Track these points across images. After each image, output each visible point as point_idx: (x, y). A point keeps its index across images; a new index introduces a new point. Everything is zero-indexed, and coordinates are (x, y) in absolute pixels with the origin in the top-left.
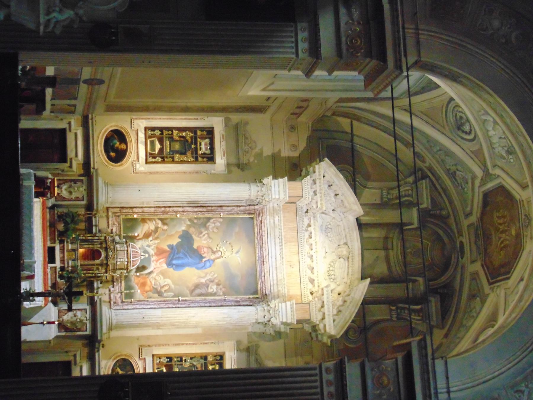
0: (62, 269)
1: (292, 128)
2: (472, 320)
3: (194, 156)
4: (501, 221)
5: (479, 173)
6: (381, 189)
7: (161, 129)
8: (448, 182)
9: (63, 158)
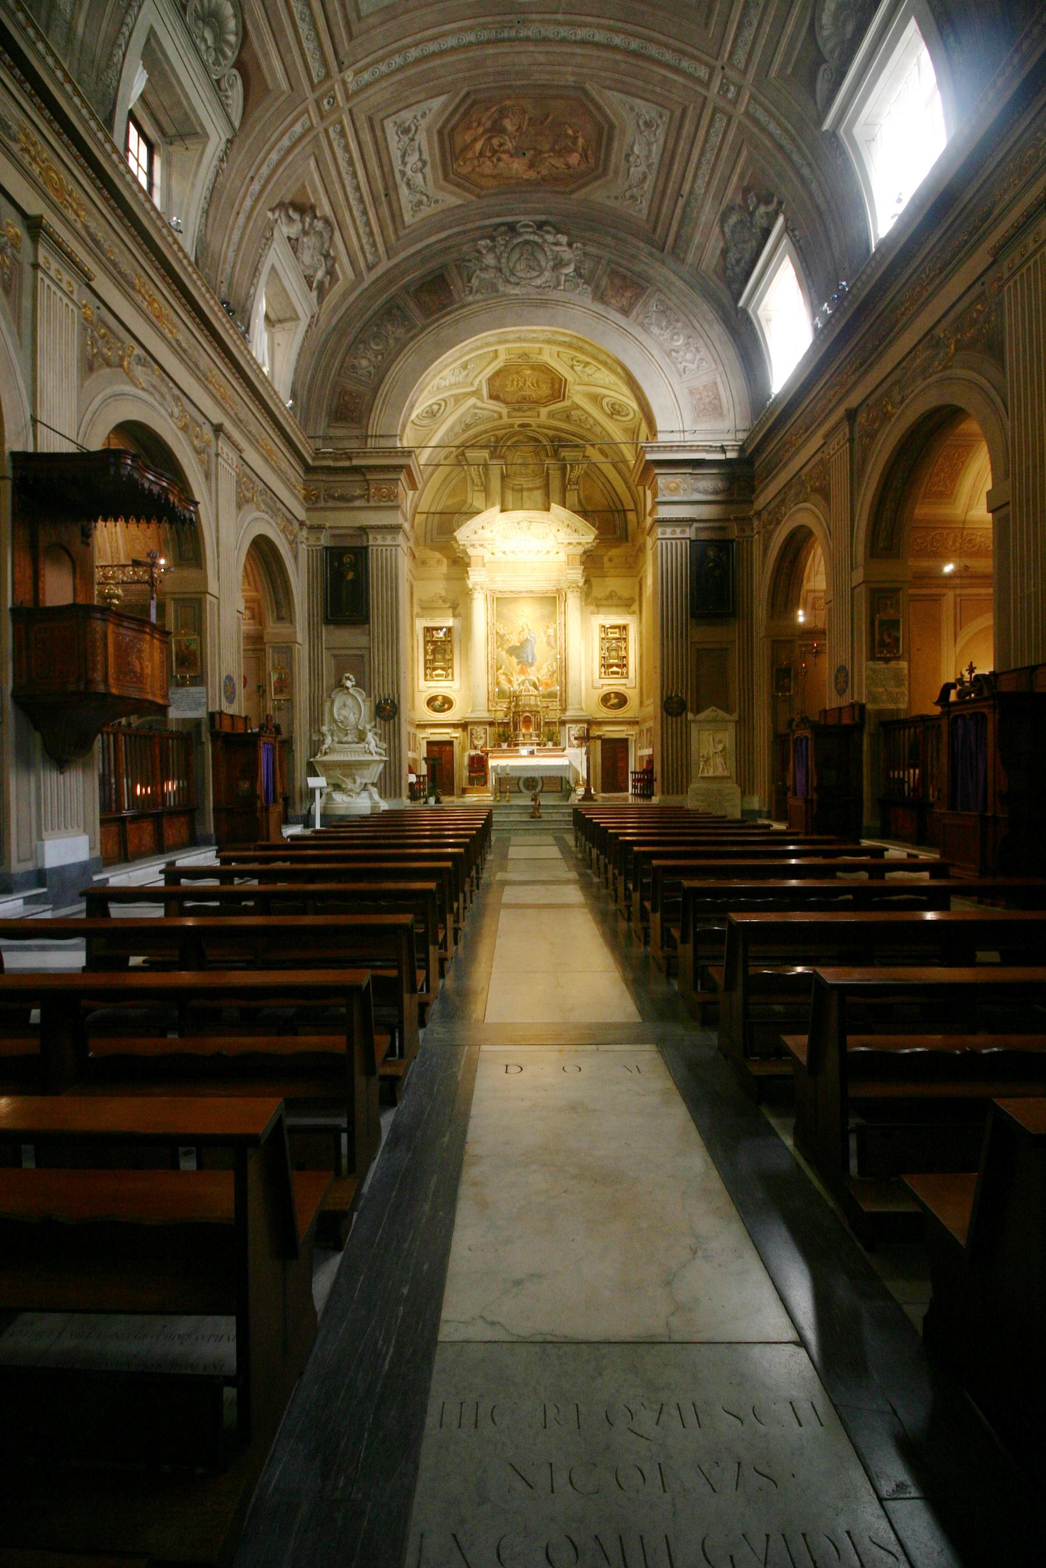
0: (538, 744)
1: (424, 563)
2: (590, 419)
4: (515, 383)
5: (473, 401)
6: (473, 491)
7: (426, 668)
8: (471, 432)
9: (450, 743)
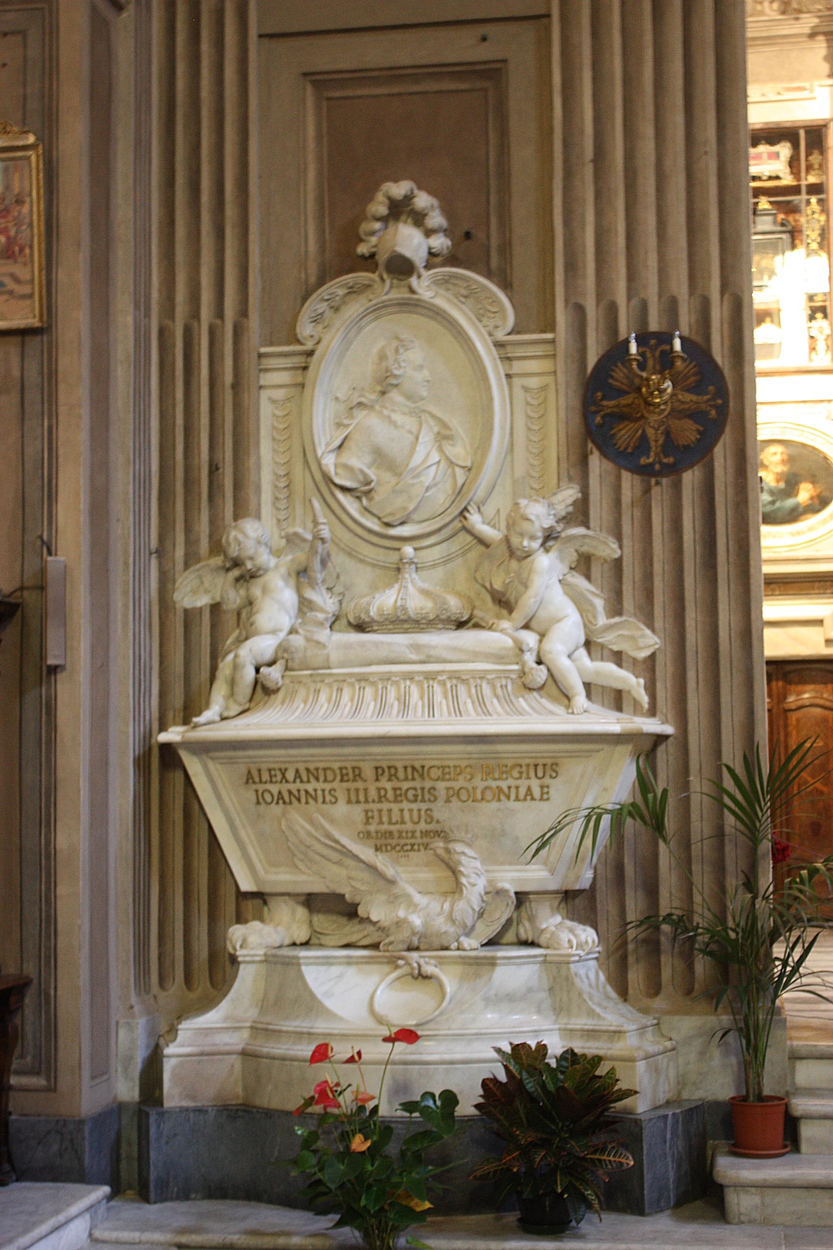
3: (804, 196)
